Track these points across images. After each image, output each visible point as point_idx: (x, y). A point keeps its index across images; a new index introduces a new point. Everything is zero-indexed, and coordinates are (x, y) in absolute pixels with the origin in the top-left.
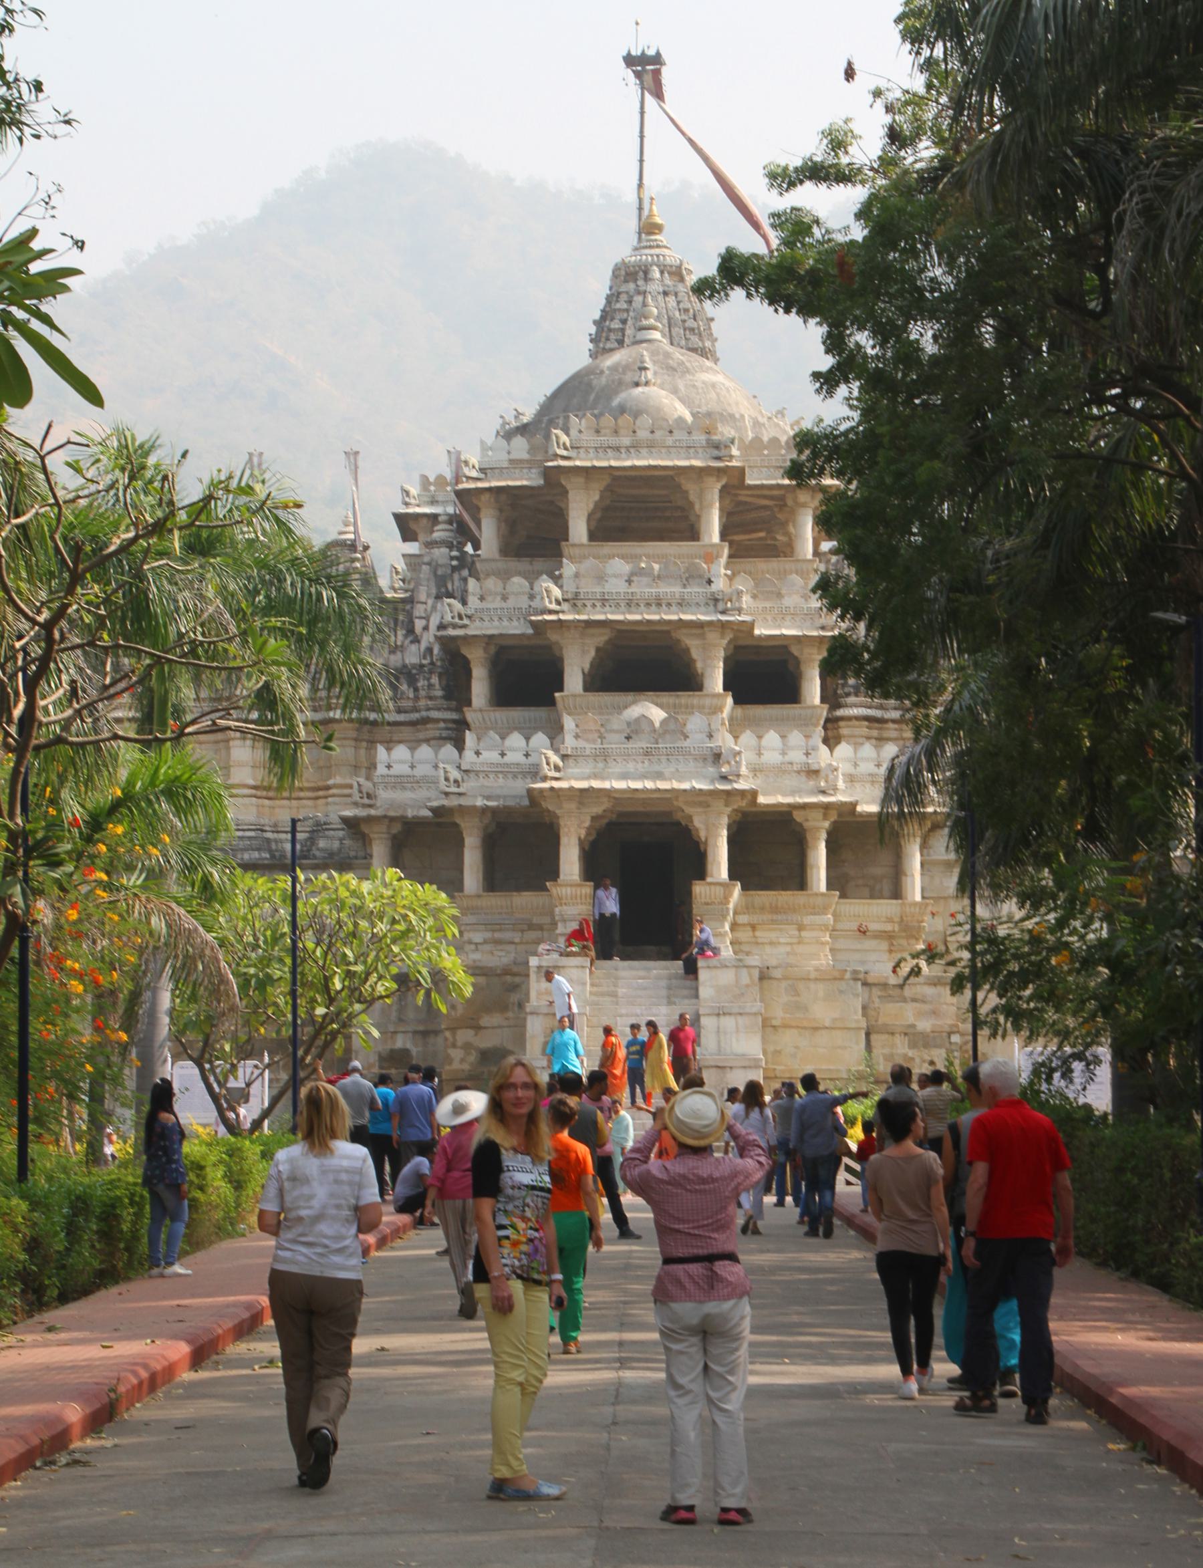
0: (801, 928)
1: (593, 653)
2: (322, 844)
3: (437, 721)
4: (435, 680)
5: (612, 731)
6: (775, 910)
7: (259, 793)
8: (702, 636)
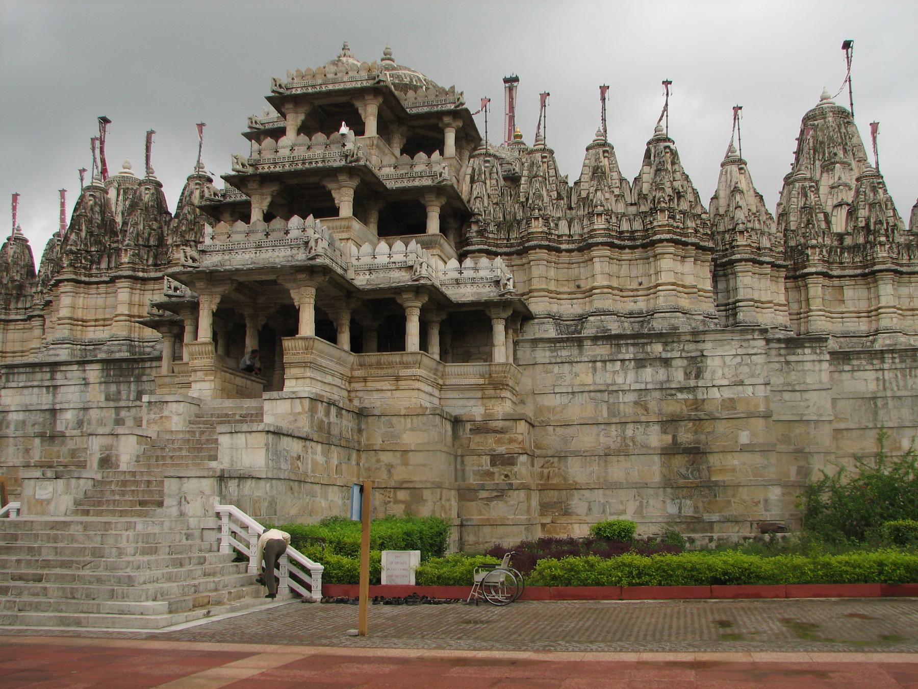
0: (398, 379)
5: (237, 232)
6: (379, 365)
8: (337, 181)
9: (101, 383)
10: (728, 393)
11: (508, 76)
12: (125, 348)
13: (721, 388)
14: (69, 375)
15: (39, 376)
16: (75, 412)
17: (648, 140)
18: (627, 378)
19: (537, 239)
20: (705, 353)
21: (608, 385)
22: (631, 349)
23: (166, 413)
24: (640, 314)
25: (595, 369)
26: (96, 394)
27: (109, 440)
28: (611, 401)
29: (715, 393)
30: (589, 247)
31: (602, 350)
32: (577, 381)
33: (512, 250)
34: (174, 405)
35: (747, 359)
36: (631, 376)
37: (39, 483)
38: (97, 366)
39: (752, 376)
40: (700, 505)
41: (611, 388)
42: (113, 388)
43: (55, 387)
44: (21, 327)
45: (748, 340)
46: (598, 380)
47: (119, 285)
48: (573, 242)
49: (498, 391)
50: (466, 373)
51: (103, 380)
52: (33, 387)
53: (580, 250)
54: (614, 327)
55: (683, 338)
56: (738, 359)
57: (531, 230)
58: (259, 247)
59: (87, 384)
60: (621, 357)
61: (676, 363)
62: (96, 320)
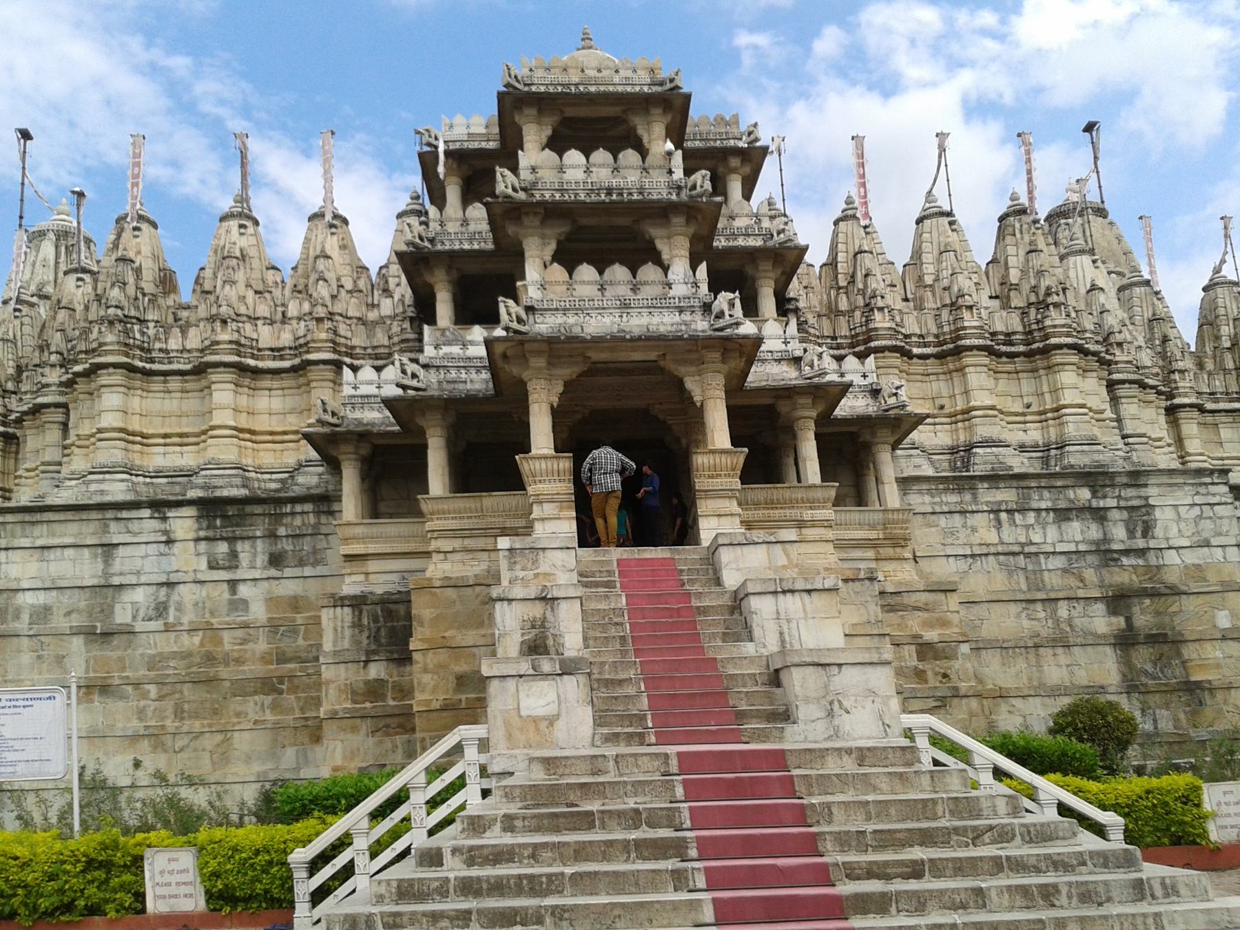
2: (300, 479)
7: (241, 435)
9: (197, 540)
10: (1191, 558)
12: (238, 481)
13: (1181, 551)
14: (134, 526)
17: (1000, 214)
18: (1048, 536)
19: (884, 338)
20: (1151, 501)
21: (1022, 545)
22: (1046, 494)
23: (544, 568)
24: (1035, 447)
25: (999, 522)
26: (189, 558)
27: (537, 610)
28: (1030, 567)
29: (1172, 558)
31: (1006, 495)
32: (976, 539)
34: (559, 554)
35: (1207, 511)
36: (1052, 533)
37: (524, 686)
38: (190, 511)
39: (1220, 534)
40: (1182, 716)
41: (1027, 550)
45: (1206, 484)
46: (1006, 539)
49: (899, 550)
50: (857, 524)
51: (202, 534)
54: (1019, 463)
55: (1118, 480)
56: (1197, 510)
57: (871, 326)
60: (1035, 505)
61: (1115, 515)
62: (166, 436)
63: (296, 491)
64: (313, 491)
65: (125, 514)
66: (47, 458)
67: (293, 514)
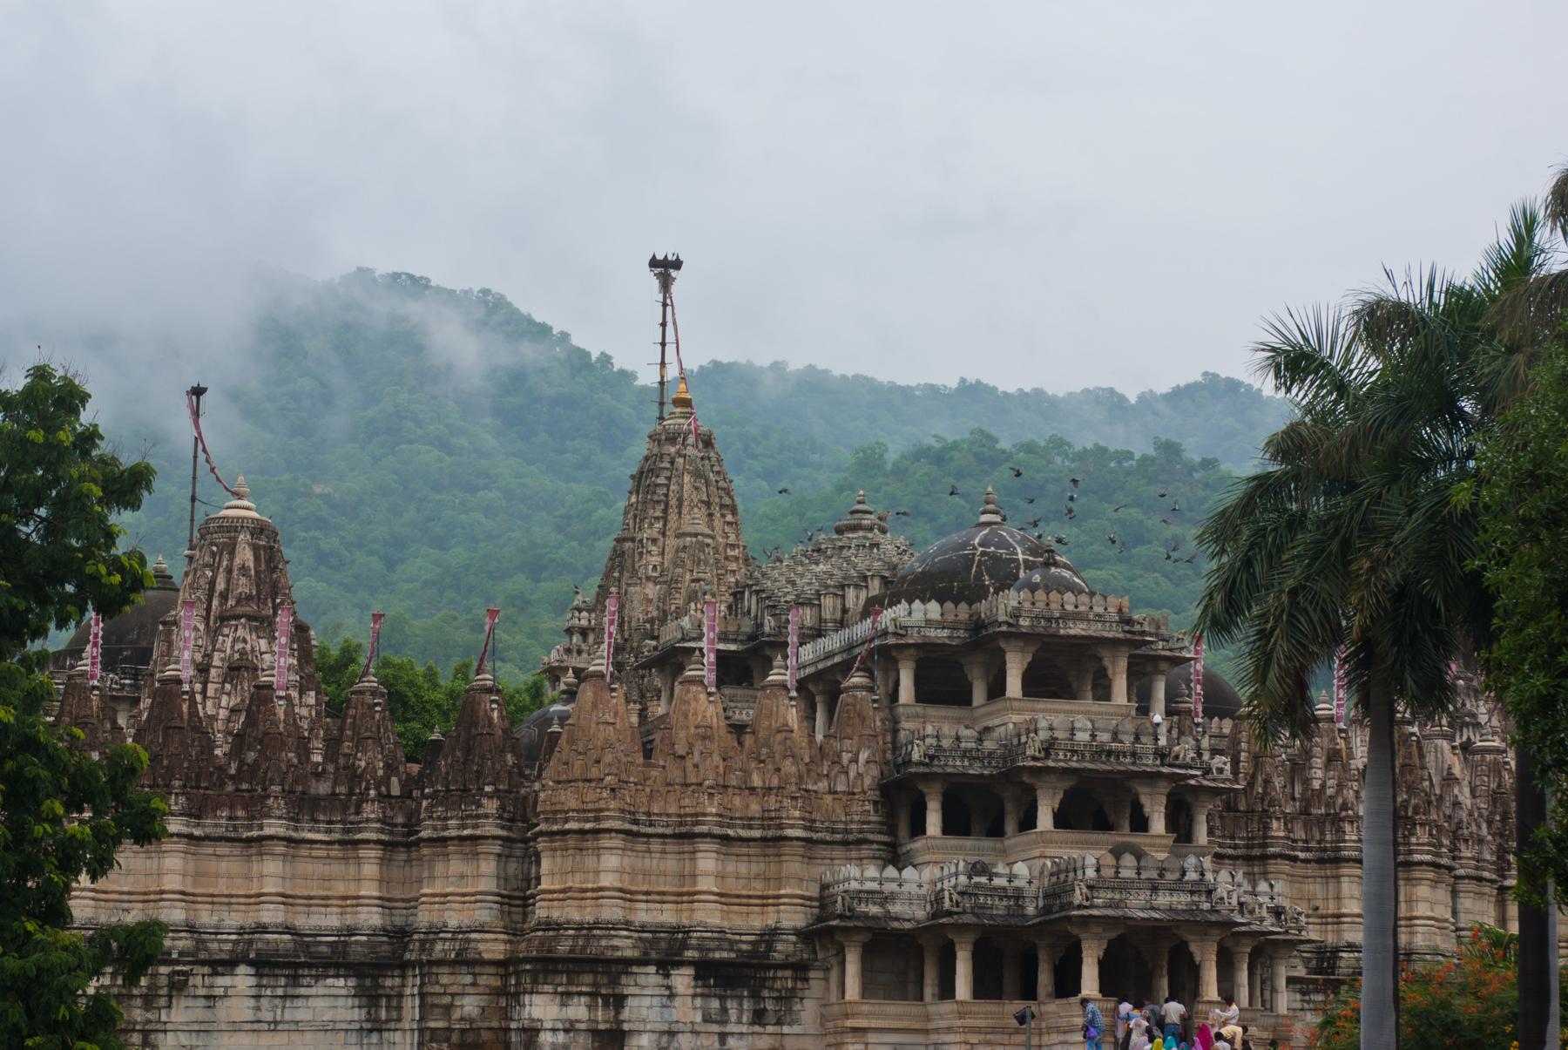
1: (1061, 796)
3: (872, 842)
4: (869, 807)
9: (694, 996)
11: (660, 257)
14: (642, 980)
15: (588, 978)
16: (655, 1037)
26: (687, 1010)
30: (1337, 861)
33: (1240, 852)
38: (690, 971)
42: (715, 1004)
43: (619, 1001)
44: (324, 853)
47: (702, 846)
48: (1308, 850)
51: (699, 990)
52: (580, 994)
53: (1320, 861)
58: (1155, 889)
59: (672, 996)
62: (647, 893)
63: (777, 957)
64: (791, 960)
65: (635, 969)
66: (481, 888)
67: (774, 979)
